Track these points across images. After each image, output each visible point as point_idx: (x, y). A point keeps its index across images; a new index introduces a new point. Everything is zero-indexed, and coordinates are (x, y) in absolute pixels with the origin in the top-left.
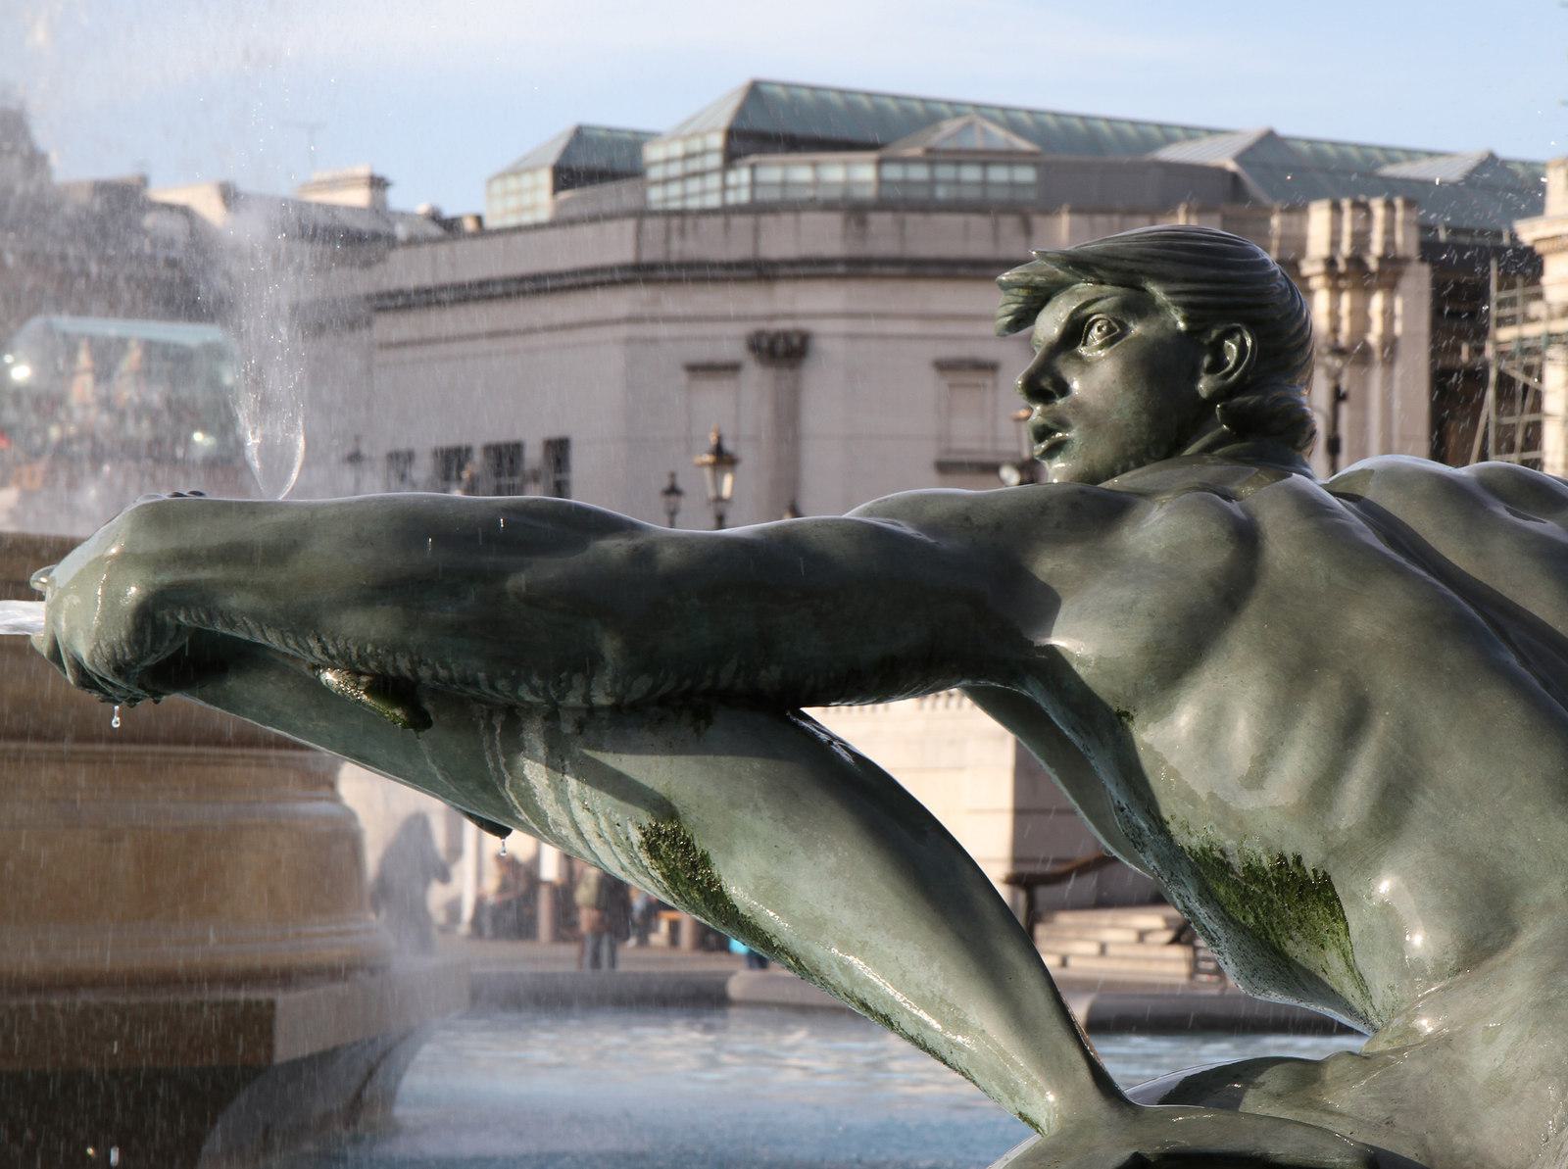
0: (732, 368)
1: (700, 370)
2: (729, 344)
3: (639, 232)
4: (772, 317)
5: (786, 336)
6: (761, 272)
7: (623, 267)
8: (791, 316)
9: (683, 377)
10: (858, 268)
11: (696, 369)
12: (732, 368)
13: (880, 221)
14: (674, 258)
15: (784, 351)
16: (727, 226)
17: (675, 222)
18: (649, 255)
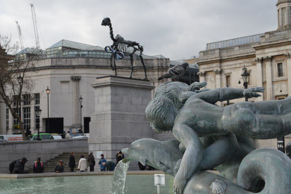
0: (68, 82)
1: (62, 82)
2: (68, 78)
3: (52, 61)
4: (75, 74)
5: (76, 77)
6: (73, 67)
7: (50, 66)
8: (78, 74)
9: (60, 83)
10: (88, 67)
11: (62, 82)
12: (68, 82)
13: (91, 60)
14: (58, 65)
15: (76, 79)
16: (66, 61)
17: (58, 59)
18: (53, 65)
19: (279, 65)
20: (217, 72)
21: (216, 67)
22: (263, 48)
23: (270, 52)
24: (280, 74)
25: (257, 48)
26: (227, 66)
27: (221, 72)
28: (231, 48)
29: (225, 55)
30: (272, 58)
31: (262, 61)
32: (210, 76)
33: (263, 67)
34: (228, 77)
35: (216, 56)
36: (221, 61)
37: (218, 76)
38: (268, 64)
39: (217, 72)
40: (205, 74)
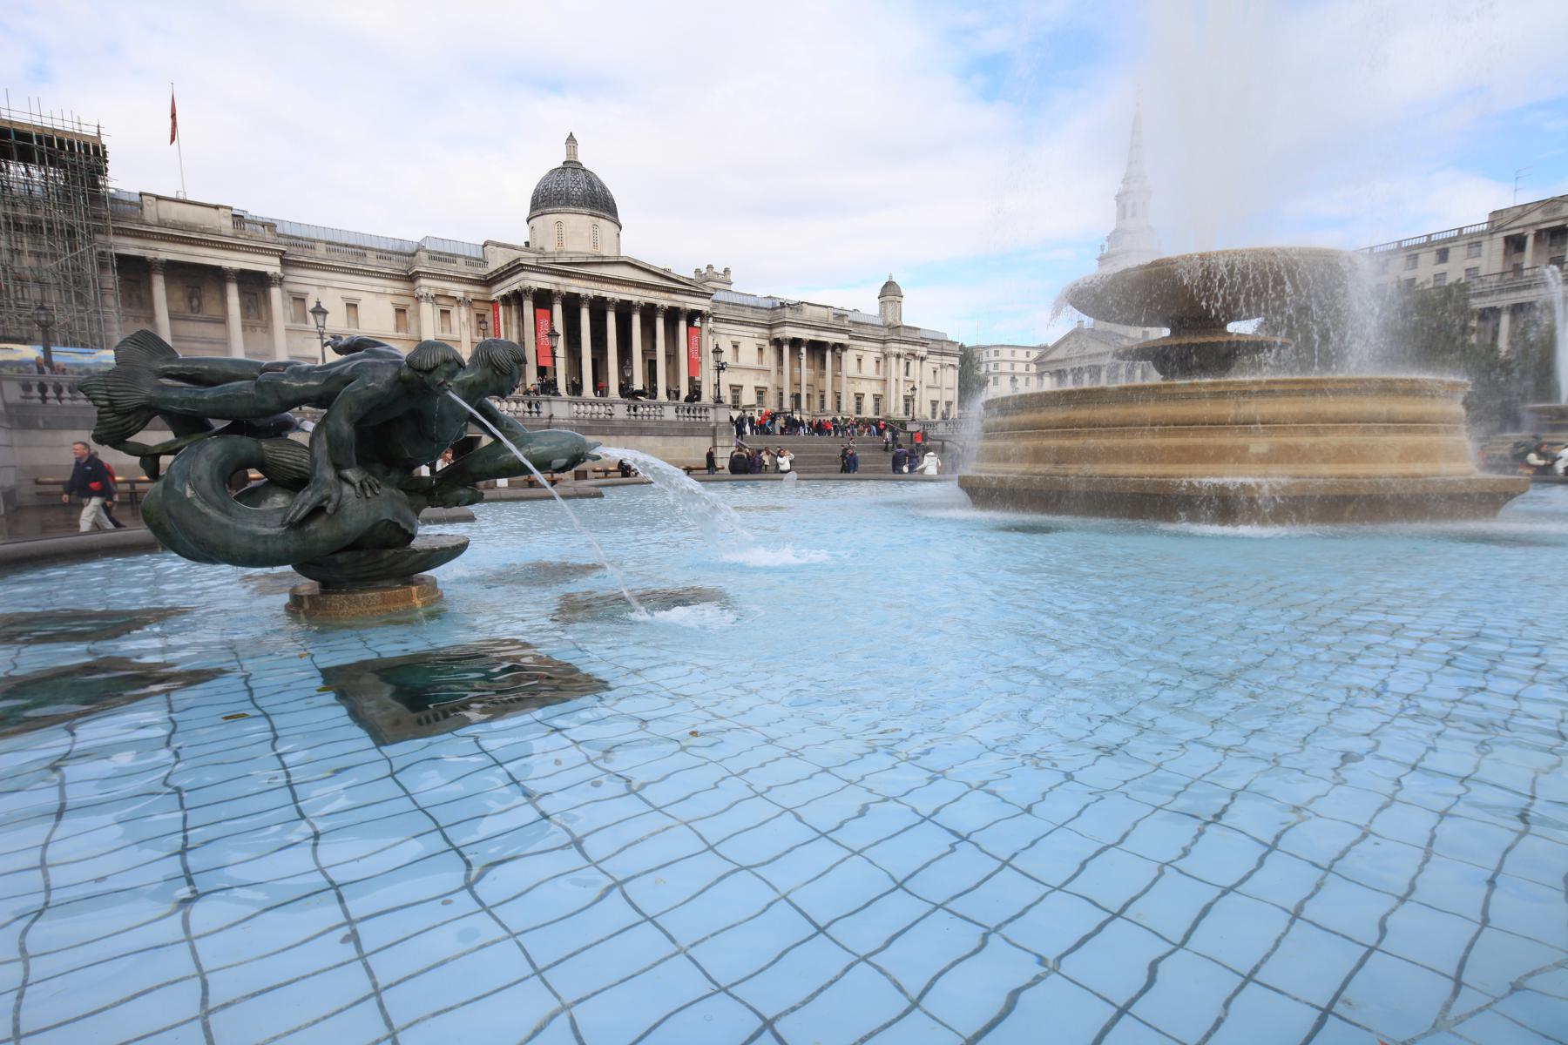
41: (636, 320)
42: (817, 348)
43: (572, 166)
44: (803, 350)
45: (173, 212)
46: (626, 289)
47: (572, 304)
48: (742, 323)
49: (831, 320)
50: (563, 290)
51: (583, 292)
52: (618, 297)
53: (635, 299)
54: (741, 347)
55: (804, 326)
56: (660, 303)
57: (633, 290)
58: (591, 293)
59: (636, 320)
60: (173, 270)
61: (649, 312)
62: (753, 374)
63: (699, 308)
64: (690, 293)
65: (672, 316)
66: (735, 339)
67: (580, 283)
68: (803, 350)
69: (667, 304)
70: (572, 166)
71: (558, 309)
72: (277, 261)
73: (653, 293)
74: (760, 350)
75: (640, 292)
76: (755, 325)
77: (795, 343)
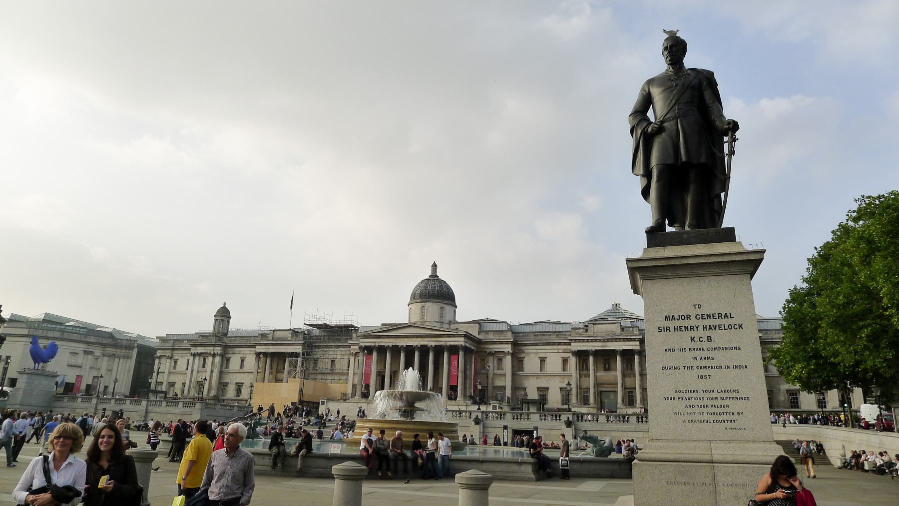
19: (205, 360)
20: (168, 357)
21: (168, 353)
22: (196, 346)
23: (200, 350)
24: (204, 366)
25: (192, 346)
26: (177, 354)
27: (171, 358)
28: (182, 341)
29: (177, 345)
30: (200, 354)
31: (194, 355)
32: (163, 360)
33: (194, 359)
34: (176, 362)
35: (170, 345)
36: (173, 349)
37: (168, 361)
38: (197, 358)
39: (168, 357)
40: (160, 357)
41: (417, 354)
42: (627, 355)
43: (434, 276)
44: (591, 358)
45: (277, 334)
46: (410, 340)
47: (382, 350)
48: (547, 344)
49: (618, 331)
50: (377, 344)
51: (386, 344)
52: (405, 344)
53: (415, 344)
54: (547, 361)
55: (588, 341)
56: (429, 344)
57: (415, 339)
58: (391, 345)
59: (417, 354)
60: (273, 355)
61: (424, 350)
62: (558, 379)
63: (456, 343)
64: (449, 336)
65: (439, 351)
66: (542, 355)
67: (387, 340)
68: (591, 358)
69: (433, 344)
70: (434, 276)
71: (375, 354)
72: (301, 347)
73: (427, 339)
74: (565, 361)
75: (419, 340)
76: (559, 344)
77: (582, 356)
